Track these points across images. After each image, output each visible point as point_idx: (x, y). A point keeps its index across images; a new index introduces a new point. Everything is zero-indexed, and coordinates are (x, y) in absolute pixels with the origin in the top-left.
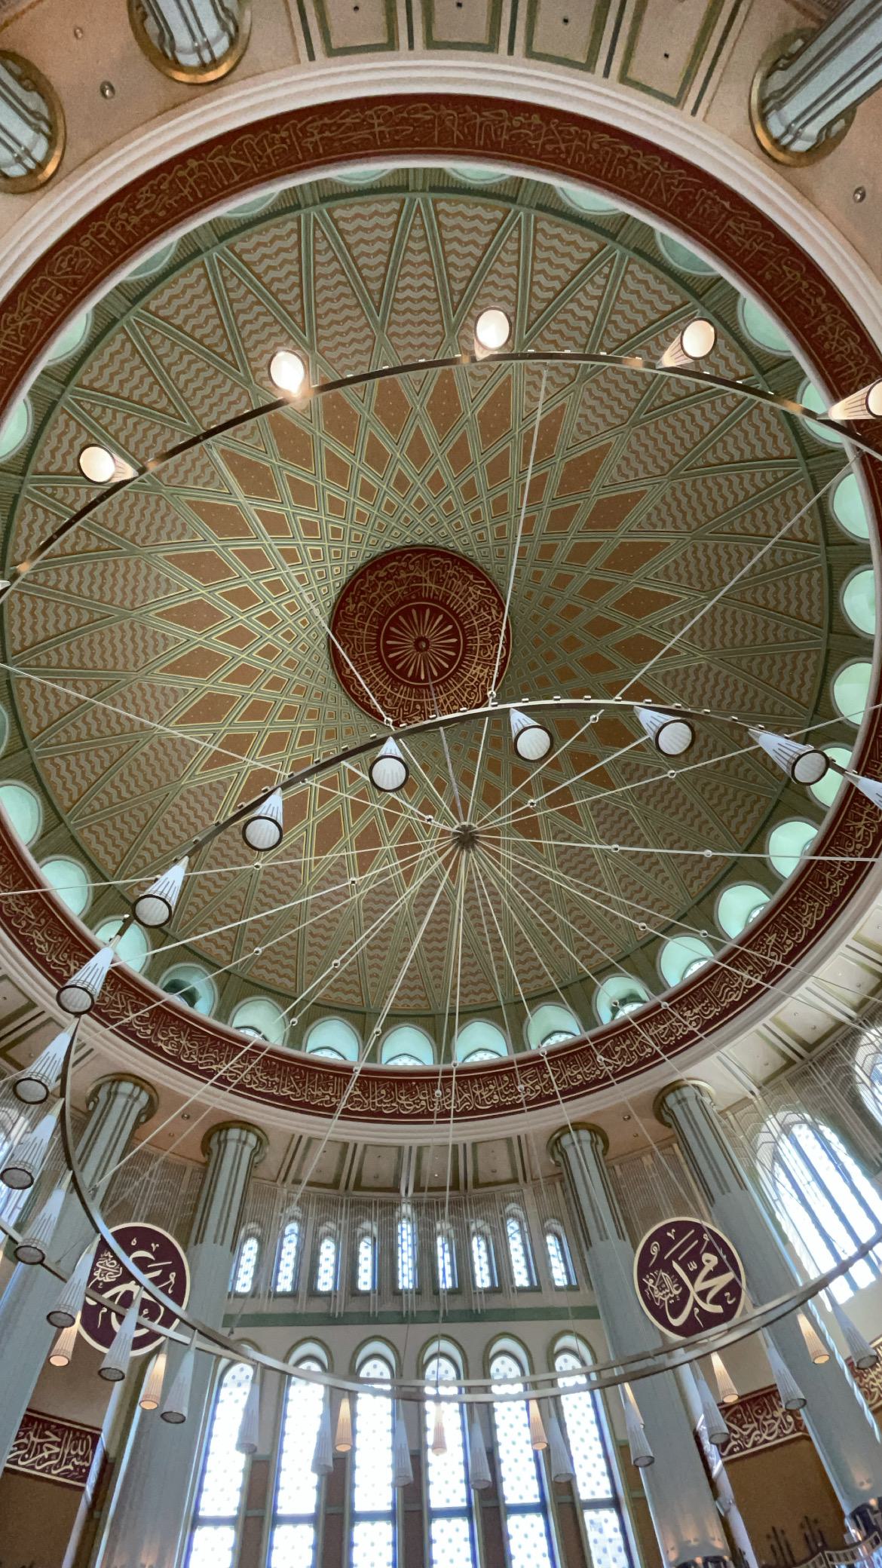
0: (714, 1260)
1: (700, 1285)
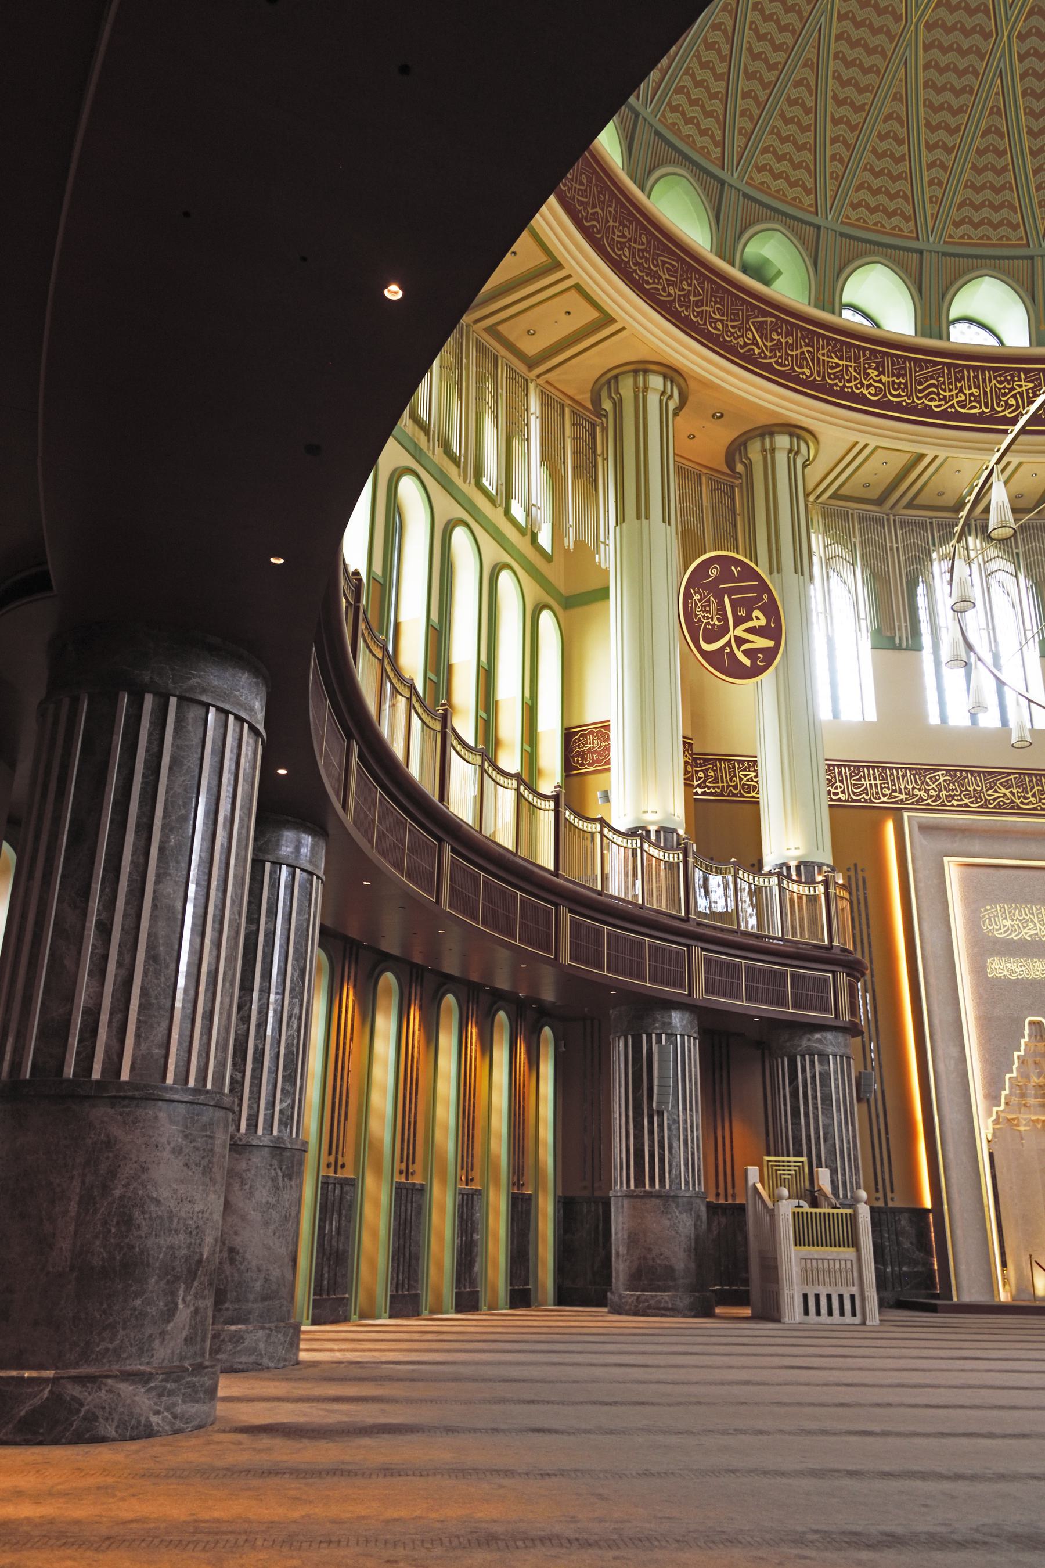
0: (763, 622)
1: (739, 632)
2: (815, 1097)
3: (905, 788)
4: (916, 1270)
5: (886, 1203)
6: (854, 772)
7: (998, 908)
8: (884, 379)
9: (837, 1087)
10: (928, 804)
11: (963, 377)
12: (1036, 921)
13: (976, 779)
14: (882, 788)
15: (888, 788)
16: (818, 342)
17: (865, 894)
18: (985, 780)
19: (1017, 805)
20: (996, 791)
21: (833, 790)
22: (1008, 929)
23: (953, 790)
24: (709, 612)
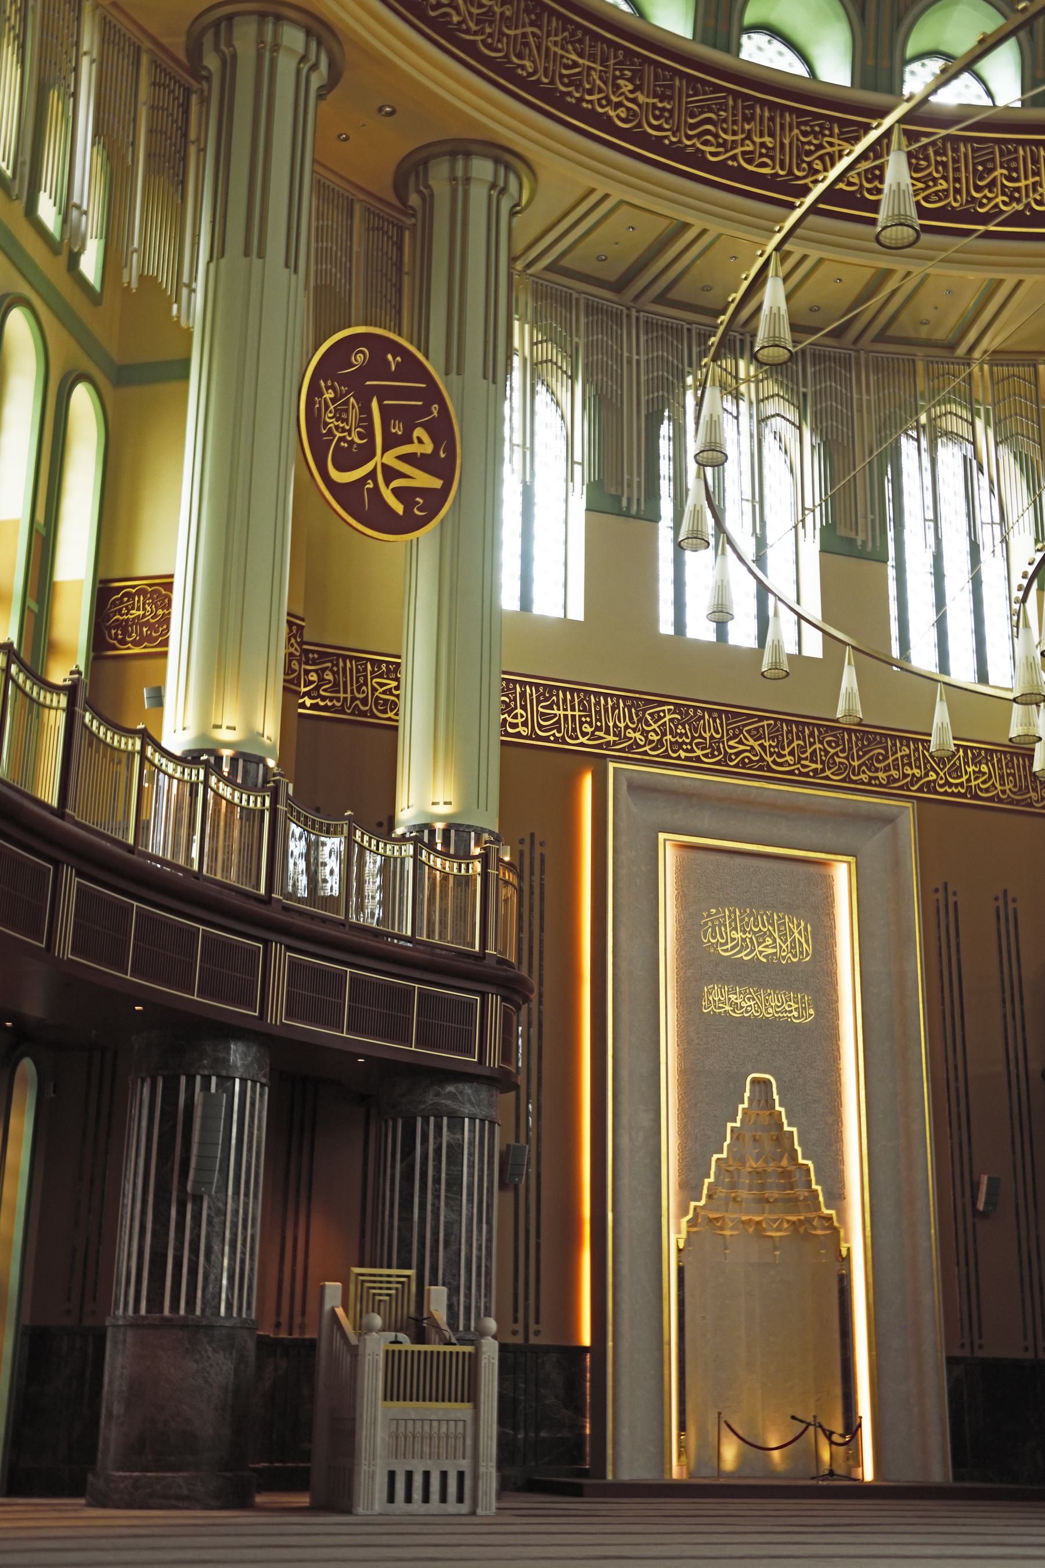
0: (428, 448)
1: (390, 459)
2: (437, 1180)
3: (615, 726)
4: (559, 1435)
5: (526, 1337)
6: (543, 694)
7: (727, 913)
8: (642, 98)
9: (471, 1166)
10: (645, 753)
11: (753, 115)
12: (776, 936)
13: (714, 721)
14: (581, 723)
15: (590, 724)
16: (549, 22)
17: (542, 879)
18: (727, 725)
19: (768, 765)
20: (740, 742)
21: (509, 719)
22: (737, 944)
23: (681, 735)
24: (346, 421)
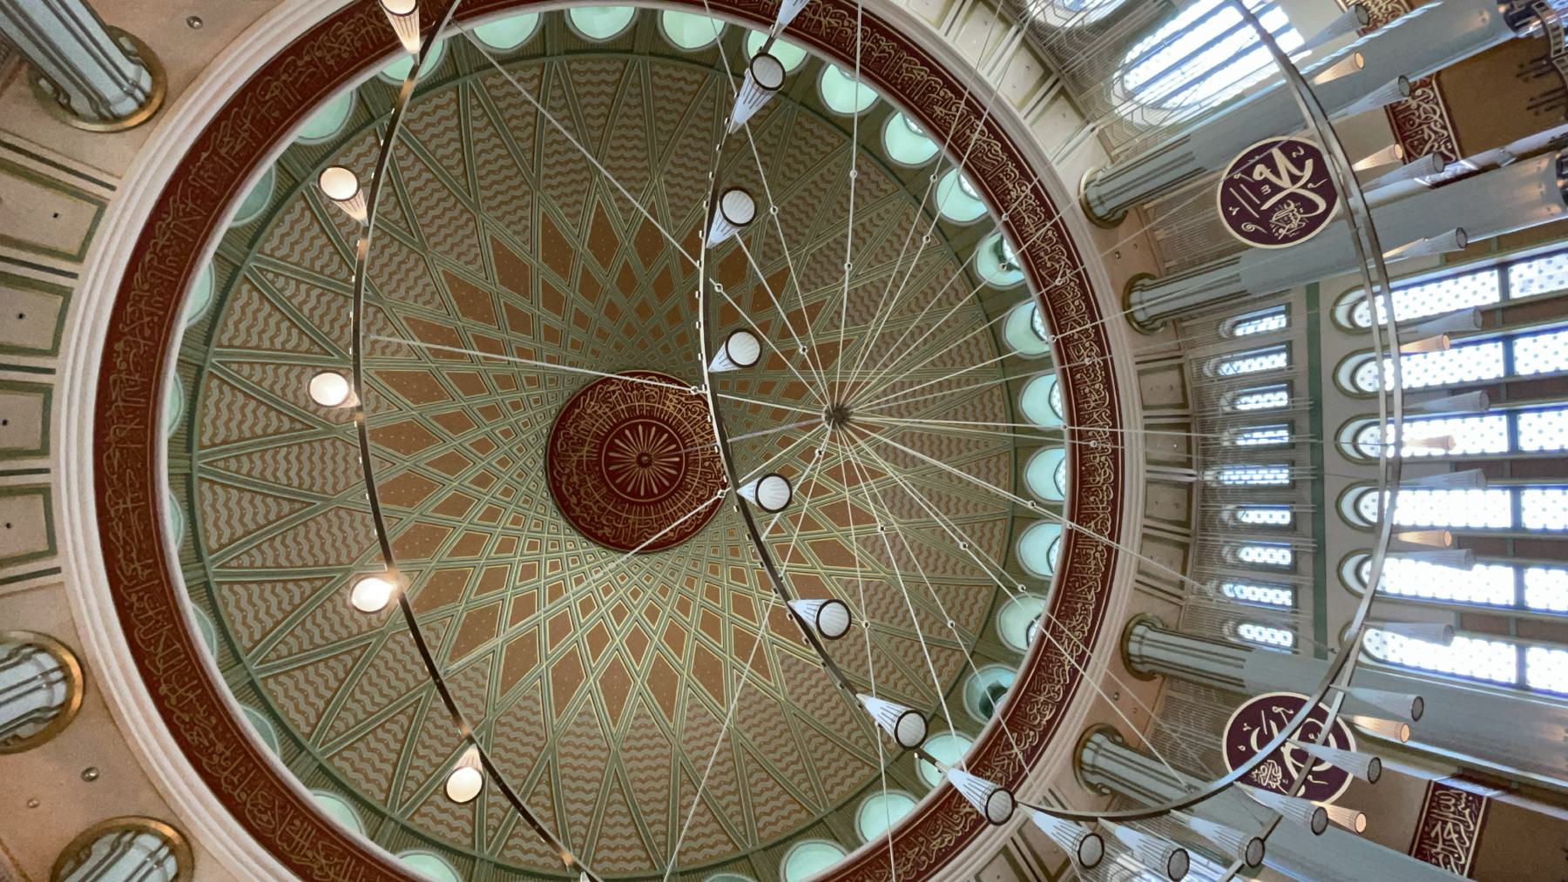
0: (1260, 168)
1: (1285, 182)
